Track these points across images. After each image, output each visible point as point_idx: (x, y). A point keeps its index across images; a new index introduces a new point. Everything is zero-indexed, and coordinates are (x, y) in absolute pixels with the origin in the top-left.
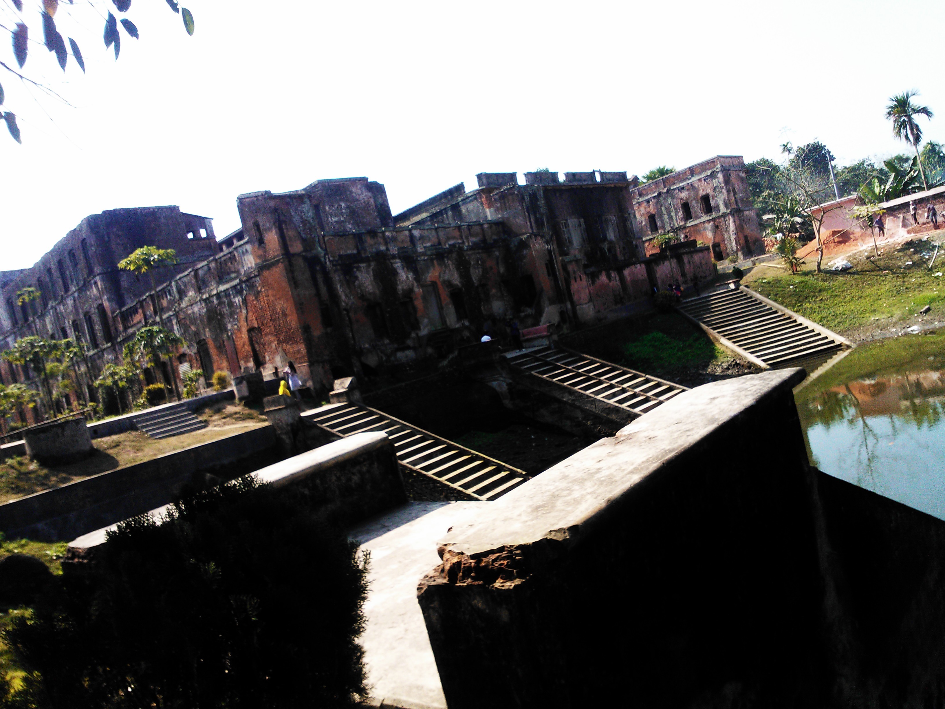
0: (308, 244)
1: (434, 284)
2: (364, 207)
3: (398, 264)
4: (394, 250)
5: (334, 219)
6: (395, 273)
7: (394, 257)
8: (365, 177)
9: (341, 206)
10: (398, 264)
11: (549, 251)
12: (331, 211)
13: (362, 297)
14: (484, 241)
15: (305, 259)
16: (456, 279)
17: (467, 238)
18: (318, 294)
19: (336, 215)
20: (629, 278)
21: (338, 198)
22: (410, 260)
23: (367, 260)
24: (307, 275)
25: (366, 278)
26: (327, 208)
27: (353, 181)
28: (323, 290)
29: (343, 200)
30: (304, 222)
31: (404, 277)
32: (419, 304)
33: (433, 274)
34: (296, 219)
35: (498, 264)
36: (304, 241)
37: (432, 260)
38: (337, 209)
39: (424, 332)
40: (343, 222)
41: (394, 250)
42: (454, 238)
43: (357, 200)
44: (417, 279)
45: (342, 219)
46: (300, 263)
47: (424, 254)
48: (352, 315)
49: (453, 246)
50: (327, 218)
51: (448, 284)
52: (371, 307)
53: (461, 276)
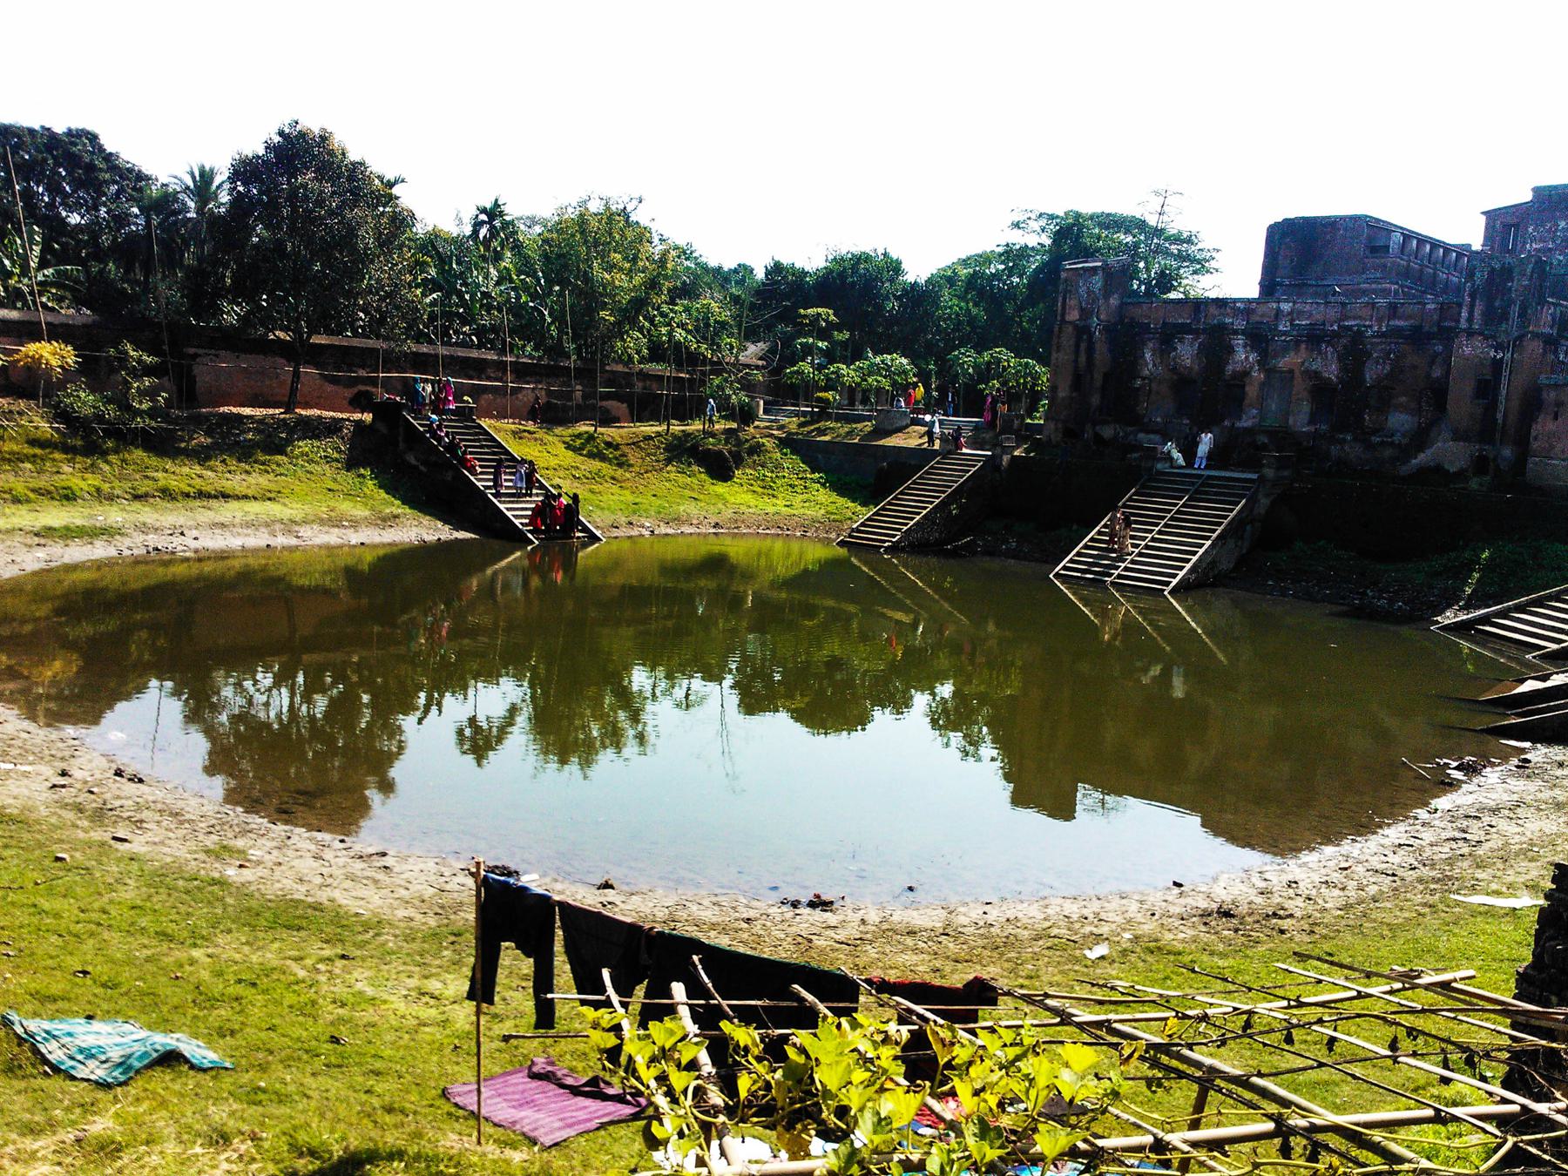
0: (1085, 313)
1: (1291, 371)
3: (1239, 341)
4: (1240, 324)
6: (1231, 350)
7: (1236, 332)
10: (1239, 341)
11: (1497, 365)
13: (1174, 370)
14: (1416, 330)
15: (1076, 327)
16: (1331, 370)
17: (1380, 320)
18: (1076, 361)
22: (1259, 338)
23: (1196, 332)
24: (1072, 342)
25: (1187, 352)
28: (1083, 359)
30: (1089, 292)
31: (1243, 355)
32: (1252, 391)
33: (1284, 362)
34: (1082, 290)
35: (1433, 362)
36: (1082, 310)
37: (1297, 343)
39: (1246, 423)
41: (1240, 324)
42: (1360, 318)
44: (1262, 363)
46: (1070, 329)
47: (1285, 333)
48: (1154, 385)
49: (1349, 328)
51: (1316, 375)
52: (1181, 383)
53: (1344, 369)
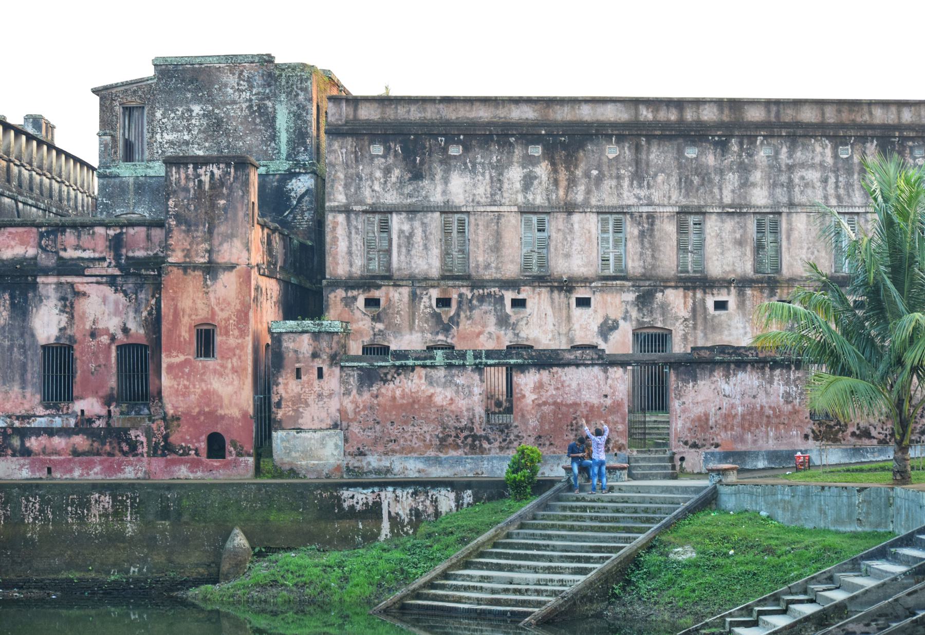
2: (246, 117)
5: (168, 137)
8: (269, 55)
9: (192, 111)
12: (165, 120)
19: (175, 129)
20: (530, 397)
21: (189, 95)
26: (158, 114)
27: (233, 62)
29: (199, 100)
38: (182, 117)
40: (187, 143)
43: (234, 102)
45: (186, 137)
50: (153, 133)
